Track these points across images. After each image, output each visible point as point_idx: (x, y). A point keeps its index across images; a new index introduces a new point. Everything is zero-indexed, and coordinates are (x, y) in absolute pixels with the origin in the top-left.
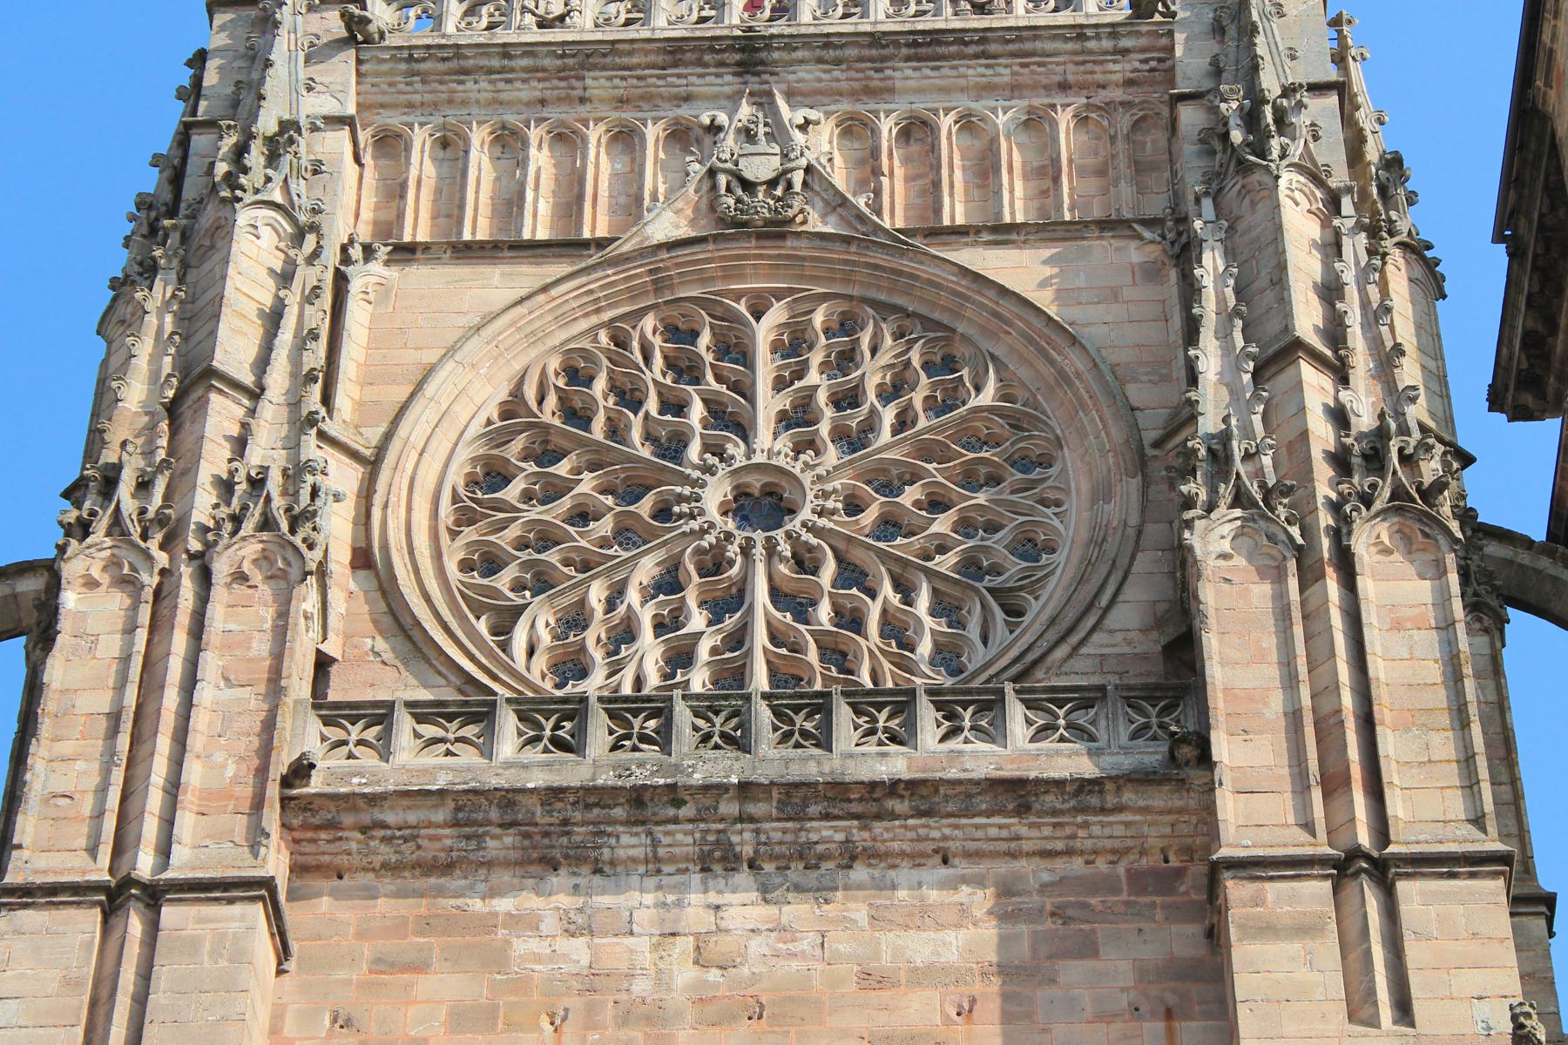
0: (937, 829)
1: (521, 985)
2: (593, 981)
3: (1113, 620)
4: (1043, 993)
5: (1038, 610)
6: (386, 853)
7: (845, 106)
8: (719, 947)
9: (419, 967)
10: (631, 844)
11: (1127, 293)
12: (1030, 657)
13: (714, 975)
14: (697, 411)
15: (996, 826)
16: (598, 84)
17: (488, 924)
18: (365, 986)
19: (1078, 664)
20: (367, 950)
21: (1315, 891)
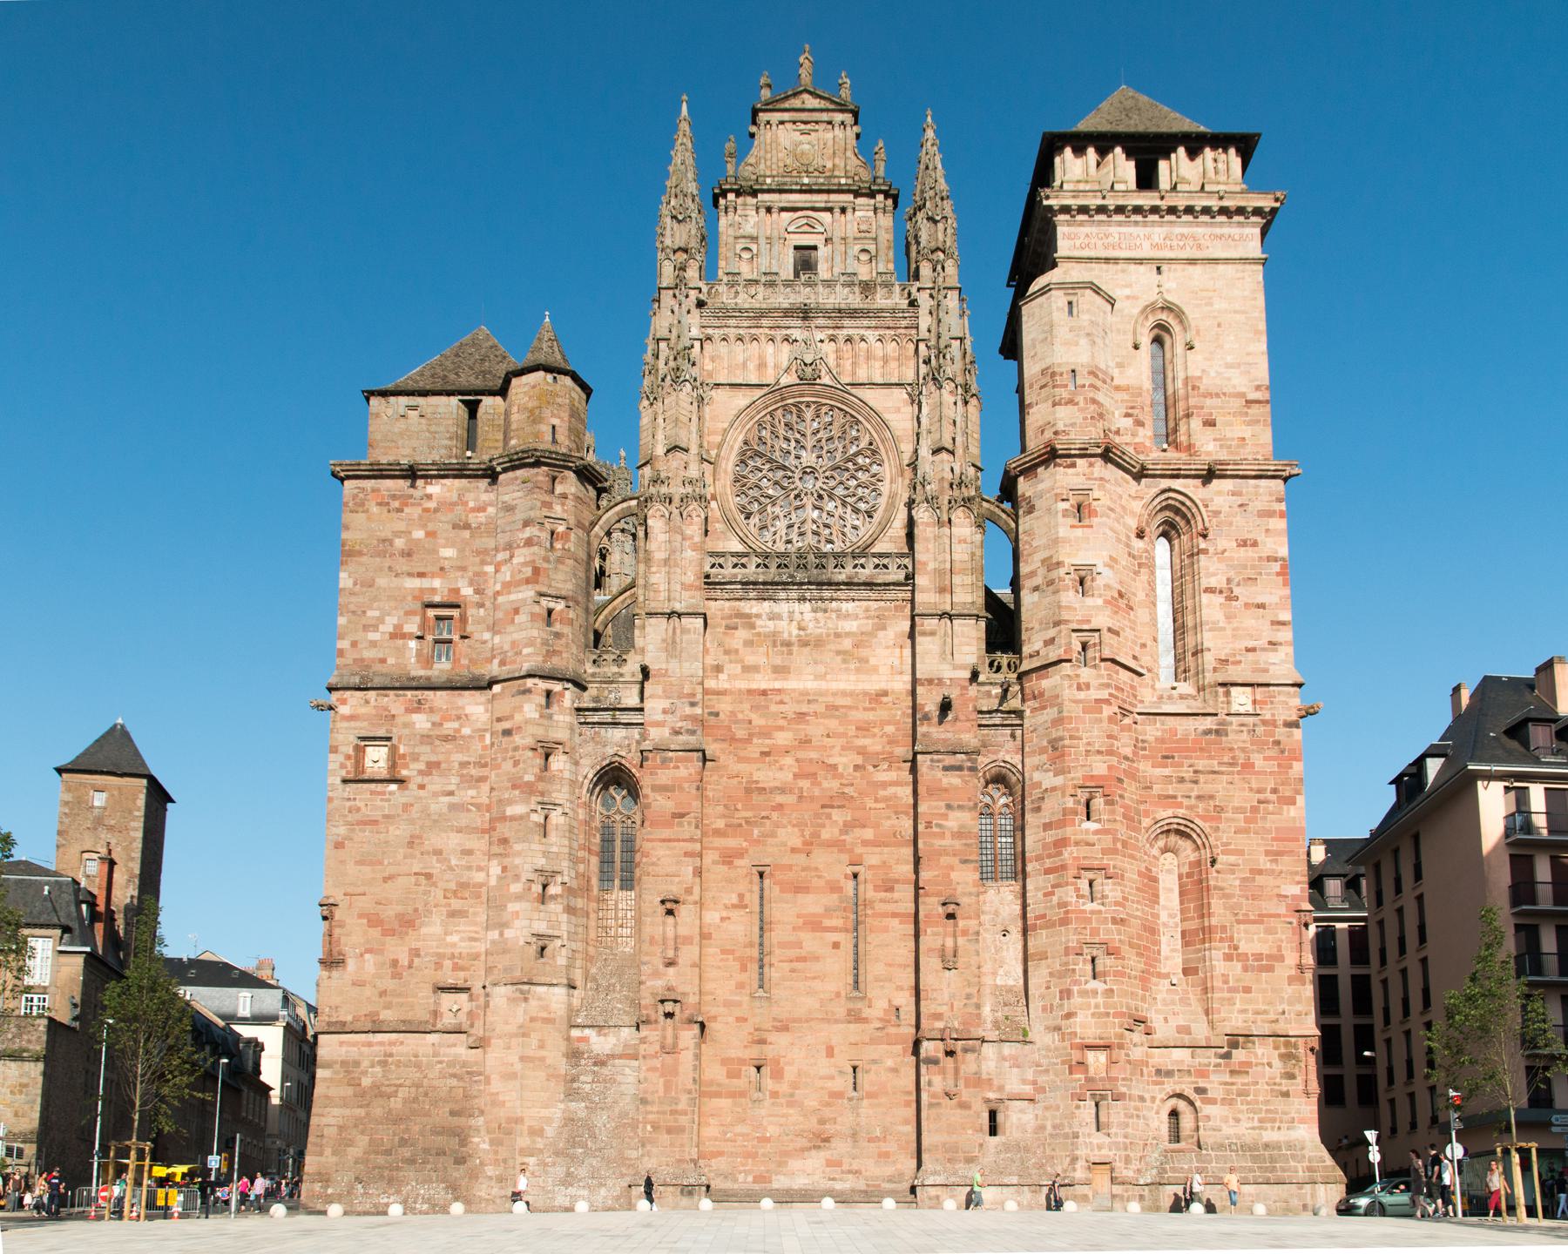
0: (852, 594)
1: (759, 634)
2: (774, 634)
3: (894, 526)
4: (875, 640)
5: (877, 516)
6: (727, 596)
7: (831, 332)
8: (803, 624)
9: (736, 628)
10: (782, 595)
11: (903, 410)
12: (874, 536)
13: (802, 633)
14: (793, 444)
15: (865, 594)
16: (764, 322)
17: (749, 616)
18: (725, 633)
19: (886, 539)
20: (724, 623)
21: (935, 621)
